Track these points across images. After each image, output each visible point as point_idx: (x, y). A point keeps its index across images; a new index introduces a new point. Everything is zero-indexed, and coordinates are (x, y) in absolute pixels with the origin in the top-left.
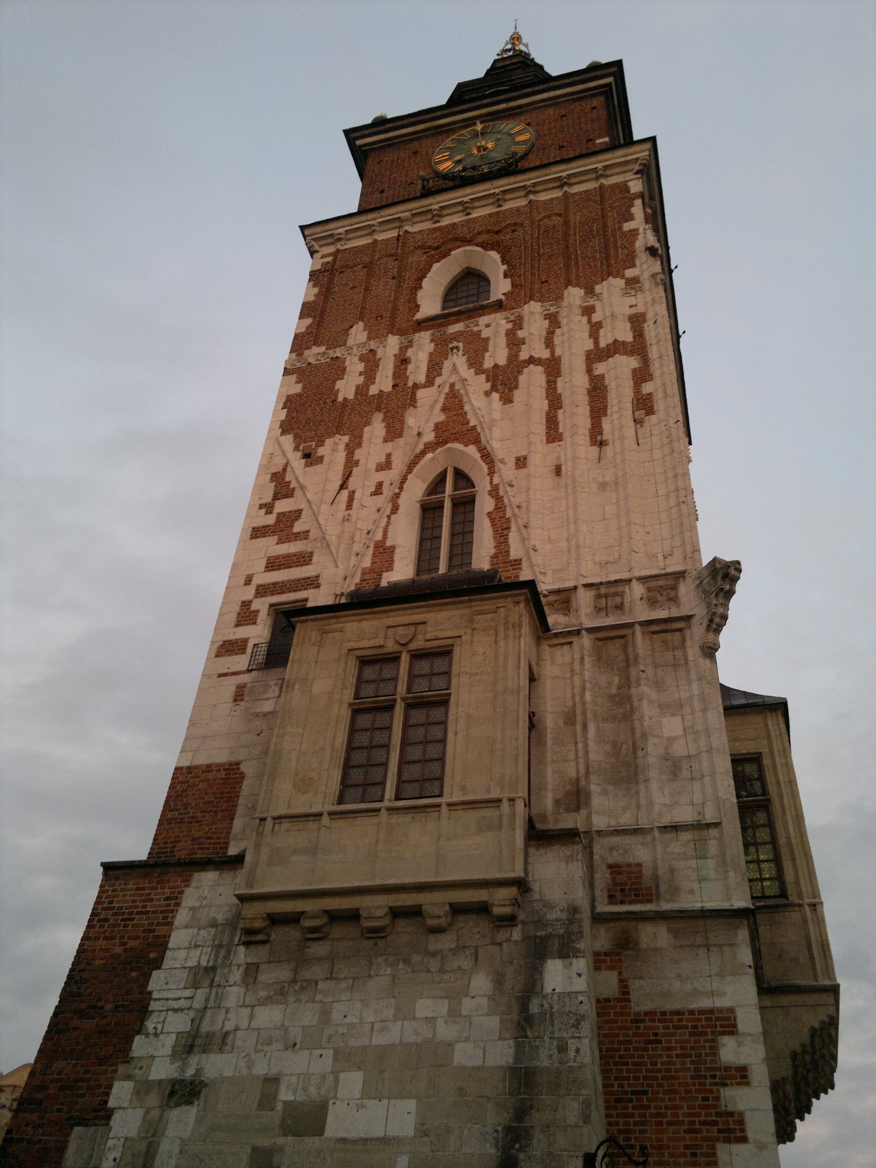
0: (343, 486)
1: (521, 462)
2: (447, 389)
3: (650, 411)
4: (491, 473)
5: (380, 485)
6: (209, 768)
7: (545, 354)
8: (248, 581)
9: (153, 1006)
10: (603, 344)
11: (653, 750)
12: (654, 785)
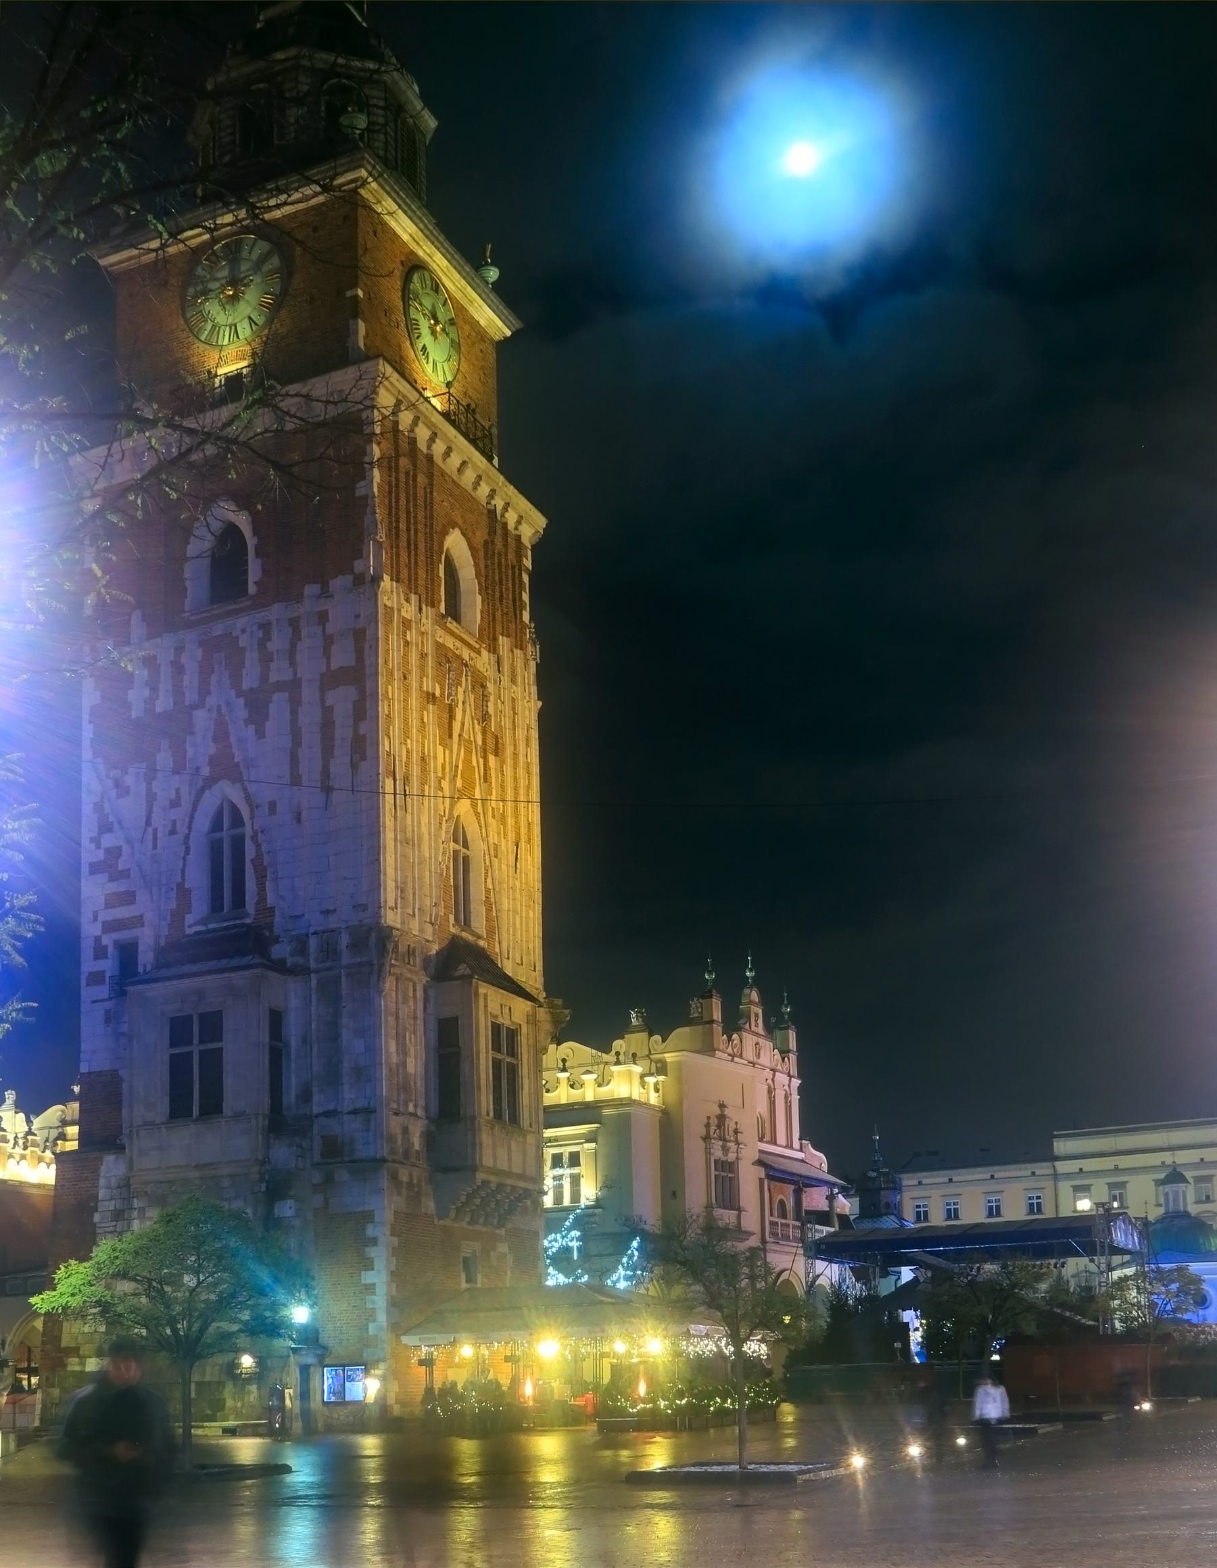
0: (148, 823)
1: (273, 806)
2: (215, 714)
3: (363, 758)
4: (252, 818)
5: (174, 823)
6: (100, 1074)
7: (287, 676)
8: (95, 919)
9: (98, 1231)
10: (332, 669)
11: (346, 1065)
12: (346, 1088)
